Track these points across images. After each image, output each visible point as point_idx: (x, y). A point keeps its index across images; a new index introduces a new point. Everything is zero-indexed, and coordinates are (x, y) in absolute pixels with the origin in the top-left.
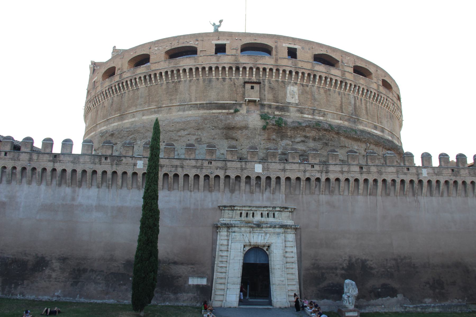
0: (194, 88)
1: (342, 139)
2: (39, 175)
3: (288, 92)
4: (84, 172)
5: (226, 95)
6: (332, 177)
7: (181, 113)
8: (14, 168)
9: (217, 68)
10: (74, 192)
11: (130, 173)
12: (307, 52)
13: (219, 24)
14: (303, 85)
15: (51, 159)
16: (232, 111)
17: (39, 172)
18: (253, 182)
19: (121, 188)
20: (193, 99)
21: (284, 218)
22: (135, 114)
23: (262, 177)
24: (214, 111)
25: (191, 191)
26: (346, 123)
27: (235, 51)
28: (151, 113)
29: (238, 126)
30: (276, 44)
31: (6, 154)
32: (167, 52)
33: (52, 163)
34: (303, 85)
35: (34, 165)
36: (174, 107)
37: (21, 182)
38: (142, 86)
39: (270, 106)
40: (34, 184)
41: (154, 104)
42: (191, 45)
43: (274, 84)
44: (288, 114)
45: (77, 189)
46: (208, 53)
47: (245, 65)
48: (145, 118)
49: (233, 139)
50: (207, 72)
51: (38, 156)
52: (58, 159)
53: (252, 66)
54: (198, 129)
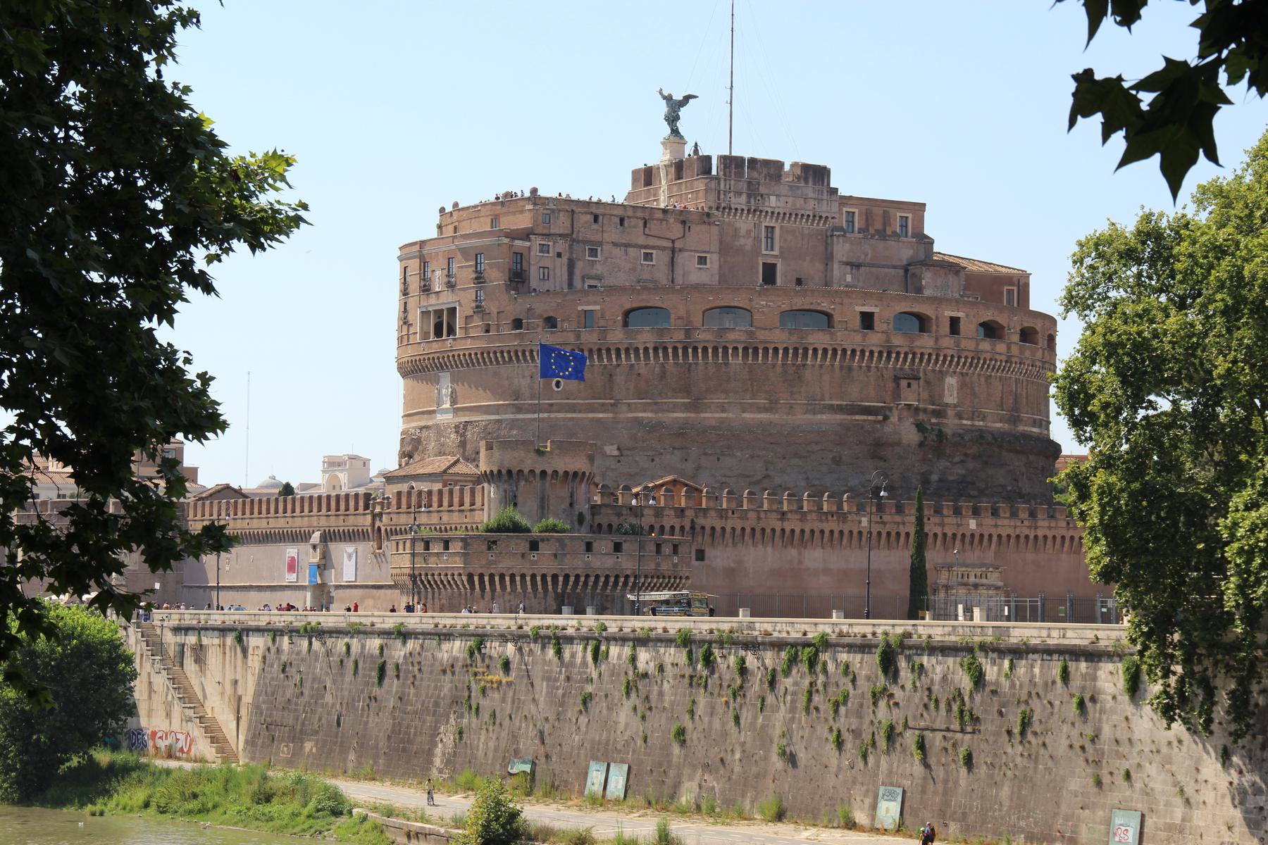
0: (826, 378)
1: (1004, 453)
4: (812, 532)
6: (1040, 533)
7: (810, 416)
8: (743, 529)
9: (863, 352)
10: (800, 554)
16: (880, 418)
18: (967, 540)
20: (827, 396)
21: (994, 578)
24: (858, 417)
26: (1006, 426)
28: (761, 409)
35: (762, 525)
38: (736, 362)
39: (925, 410)
44: (945, 421)
48: (746, 415)
49: (881, 458)
53: (906, 349)
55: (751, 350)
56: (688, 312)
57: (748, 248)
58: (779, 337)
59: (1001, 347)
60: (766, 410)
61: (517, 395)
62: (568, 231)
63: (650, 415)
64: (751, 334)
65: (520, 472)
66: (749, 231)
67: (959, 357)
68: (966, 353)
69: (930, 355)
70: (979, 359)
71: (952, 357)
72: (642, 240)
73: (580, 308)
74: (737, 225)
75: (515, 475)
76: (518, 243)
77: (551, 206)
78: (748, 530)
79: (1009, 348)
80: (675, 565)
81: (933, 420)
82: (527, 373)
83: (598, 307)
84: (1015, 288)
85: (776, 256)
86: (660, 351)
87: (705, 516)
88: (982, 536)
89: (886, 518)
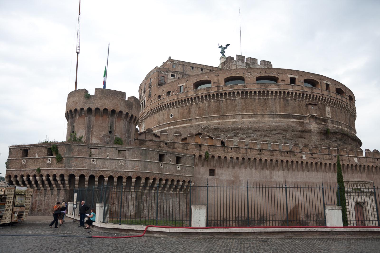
0: (277, 104)
1: (350, 140)
2: (252, 163)
3: (326, 110)
4: (277, 161)
5: (298, 111)
7: (272, 119)
9: (292, 93)
10: (271, 173)
11: (300, 162)
12: (333, 87)
13: (225, 46)
14: (332, 106)
15: (258, 153)
17: (252, 161)
18: (354, 168)
19: (294, 171)
20: (278, 111)
22: (235, 116)
23: (358, 165)
25: (327, 172)
27: (301, 83)
28: (250, 117)
29: (307, 130)
30: (320, 81)
31: (231, 149)
32: (258, 79)
33: (259, 155)
34: (332, 106)
36: (266, 115)
37: (240, 167)
38: (239, 98)
39: (319, 119)
40: (248, 169)
41: (251, 111)
42: (275, 76)
43: (320, 105)
45: (272, 171)
46: (286, 83)
47: (307, 93)
48: (244, 120)
49: (303, 138)
50: (286, 95)
51: (251, 151)
52: (262, 152)
53: (310, 93)
54: (285, 131)
55: (244, 93)
56: (218, 80)
58: (256, 87)
60: (252, 117)
61: (159, 123)
62: (182, 71)
63: (204, 122)
64: (245, 86)
65: (76, 110)
67: (331, 99)
68: (333, 98)
69: (320, 96)
70: (338, 101)
71: (328, 98)
73: (178, 86)
75: (74, 114)
76: (162, 72)
77: (176, 62)
79: (346, 101)
80: (177, 171)
81: (323, 123)
82: (162, 114)
83: (184, 84)
86: (207, 96)
87: (214, 150)
88: (360, 166)
89: (314, 156)
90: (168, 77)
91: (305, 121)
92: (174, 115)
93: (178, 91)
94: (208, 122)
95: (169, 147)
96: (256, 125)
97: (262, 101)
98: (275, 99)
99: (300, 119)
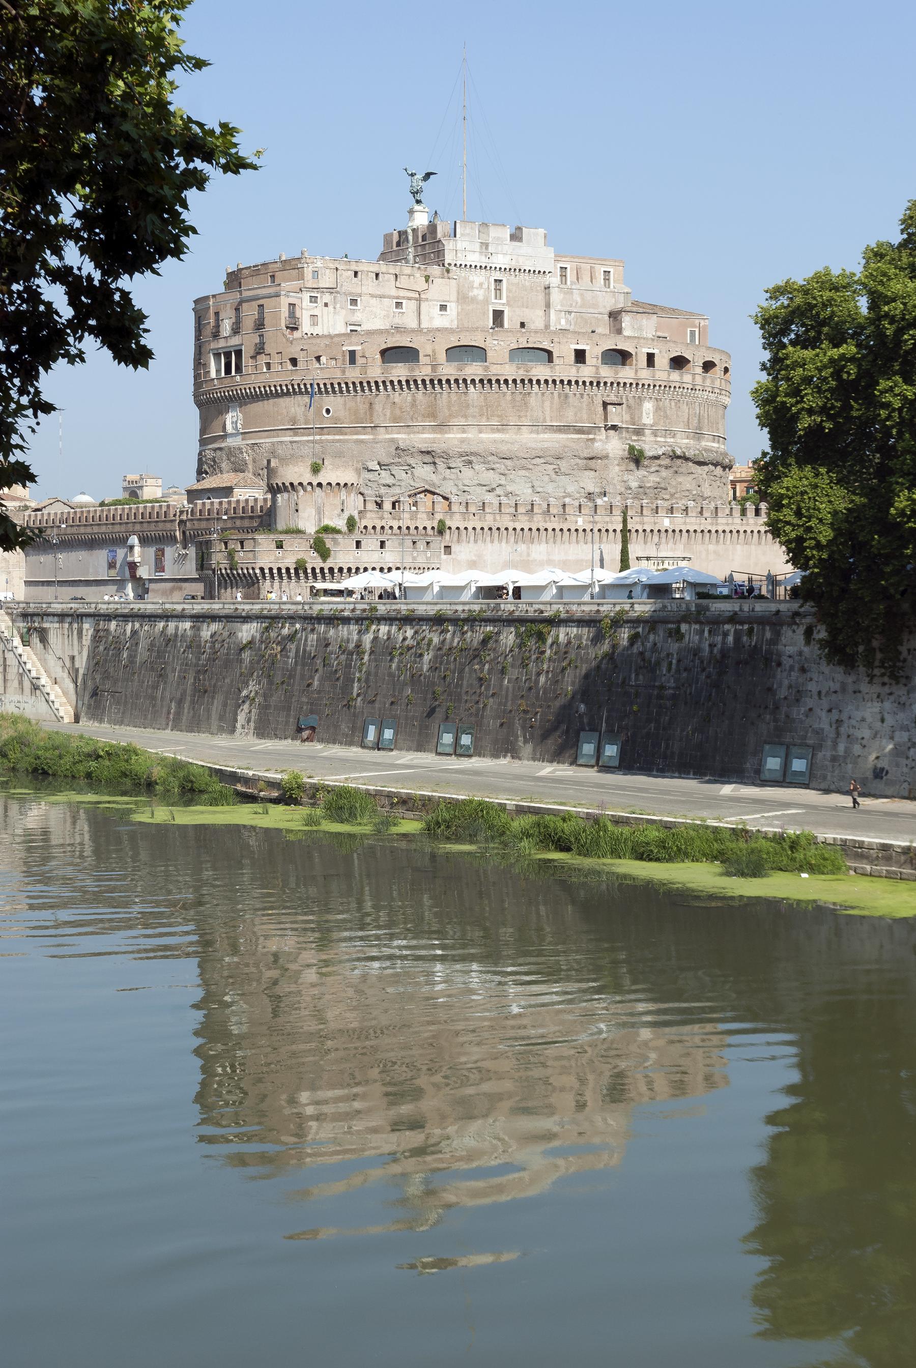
0: (547, 404)
5: (585, 416)
7: (534, 436)
10: (528, 548)
12: (663, 357)
14: (656, 399)
20: (548, 418)
28: (493, 431)
34: (656, 399)
41: (496, 419)
43: (631, 401)
44: (644, 438)
47: (606, 380)
57: (481, 298)
58: (510, 371)
59: (687, 378)
60: (498, 431)
61: (294, 421)
64: (486, 369)
66: (481, 284)
72: (394, 292)
73: (344, 348)
74: (471, 278)
78: (486, 529)
84: (697, 330)
85: (503, 304)
88: (674, 531)
90: (304, 304)
91: (598, 437)
92: (335, 412)
93: (344, 360)
94: (412, 436)
95: (394, 519)
96: (504, 448)
97: (519, 398)
98: (543, 394)
99: (589, 433)
